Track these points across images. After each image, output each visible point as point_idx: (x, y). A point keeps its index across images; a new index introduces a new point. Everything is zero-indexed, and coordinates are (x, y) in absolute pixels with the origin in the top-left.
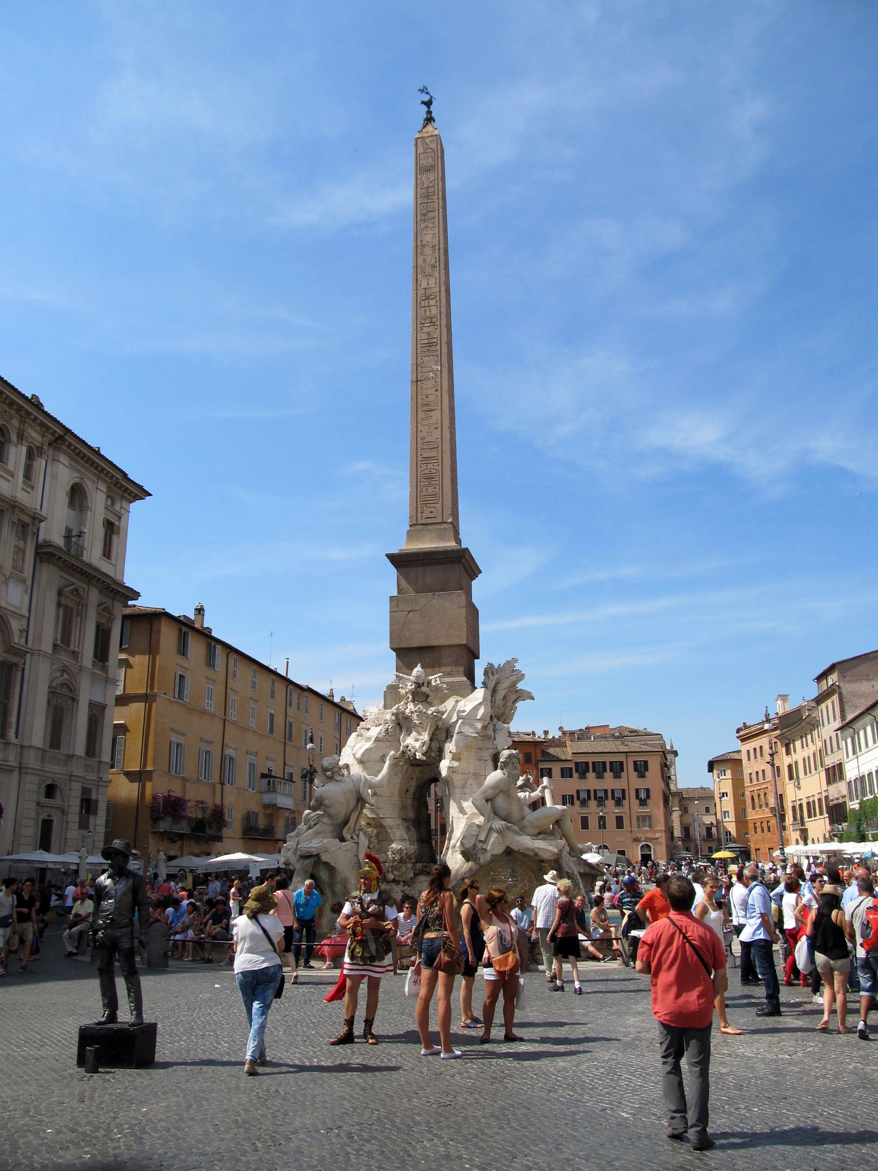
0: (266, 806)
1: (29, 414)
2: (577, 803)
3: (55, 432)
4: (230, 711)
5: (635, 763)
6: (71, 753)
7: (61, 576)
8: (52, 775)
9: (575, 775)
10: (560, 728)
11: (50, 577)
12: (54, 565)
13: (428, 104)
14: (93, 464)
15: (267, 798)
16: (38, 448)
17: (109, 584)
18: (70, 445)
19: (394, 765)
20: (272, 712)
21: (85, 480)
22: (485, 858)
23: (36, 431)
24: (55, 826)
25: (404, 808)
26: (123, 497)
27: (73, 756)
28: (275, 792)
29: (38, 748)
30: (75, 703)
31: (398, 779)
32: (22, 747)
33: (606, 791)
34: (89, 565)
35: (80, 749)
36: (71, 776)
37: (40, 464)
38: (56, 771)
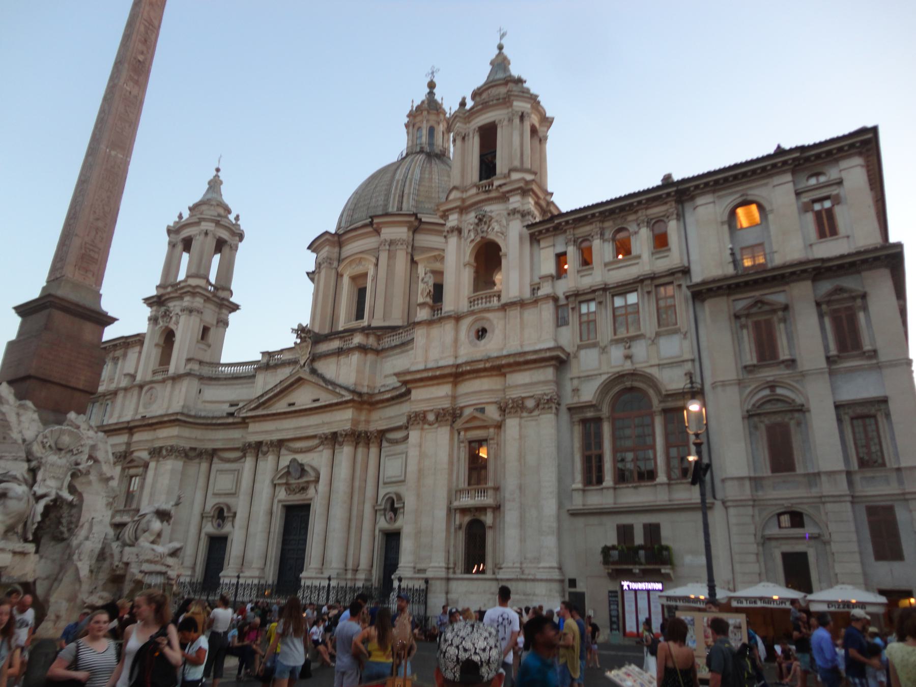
1: (631, 205)
3: (668, 194)
6: (816, 471)
7: (734, 300)
8: (783, 502)
12: (711, 297)
14: (744, 175)
16: (664, 216)
17: (814, 269)
18: (697, 187)
21: (750, 192)
23: (656, 206)
27: (818, 474)
29: (741, 479)
30: (807, 414)
32: (723, 481)
36: (821, 497)
37: (672, 227)
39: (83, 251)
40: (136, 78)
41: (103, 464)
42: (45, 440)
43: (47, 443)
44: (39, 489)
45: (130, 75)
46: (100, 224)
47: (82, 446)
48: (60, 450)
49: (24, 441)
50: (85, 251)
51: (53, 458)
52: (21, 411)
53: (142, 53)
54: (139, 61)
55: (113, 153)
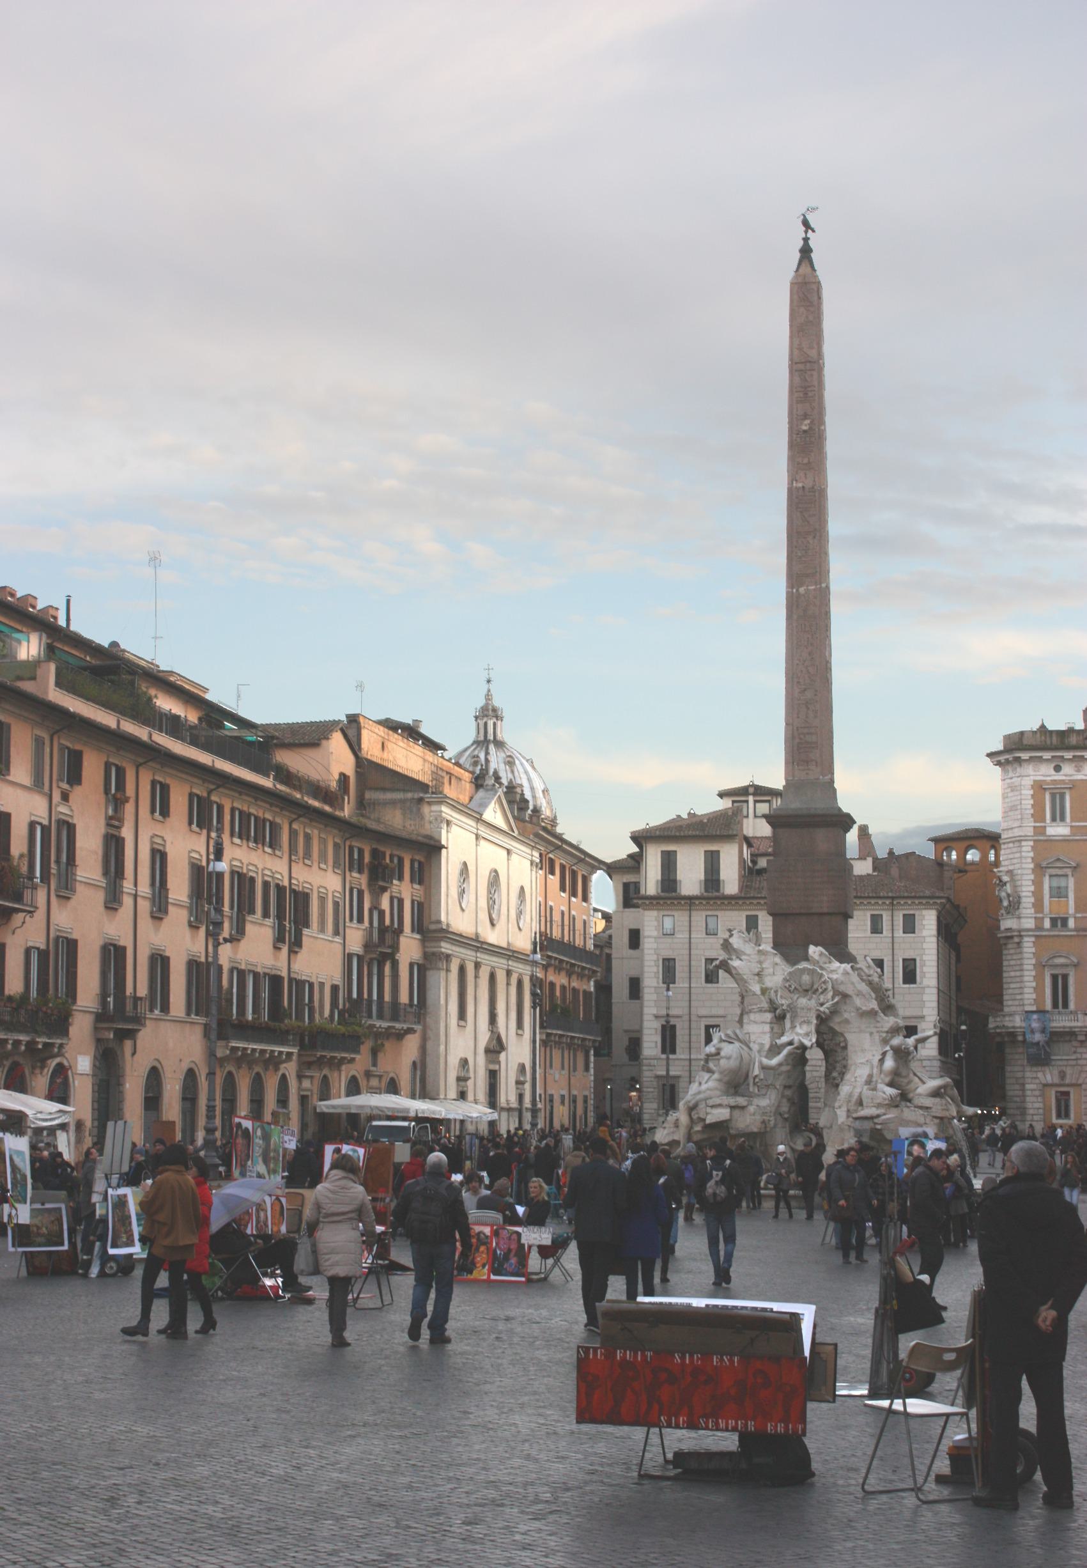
39: (797, 740)
40: (806, 461)
41: (854, 997)
42: (787, 985)
43: (790, 986)
44: (784, 1039)
45: (798, 463)
46: (809, 694)
47: (825, 982)
48: (807, 991)
49: (764, 991)
50: (801, 739)
51: (803, 1001)
52: (763, 958)
53: (805, 416)
54: (805, 431)
55: (802, 590)
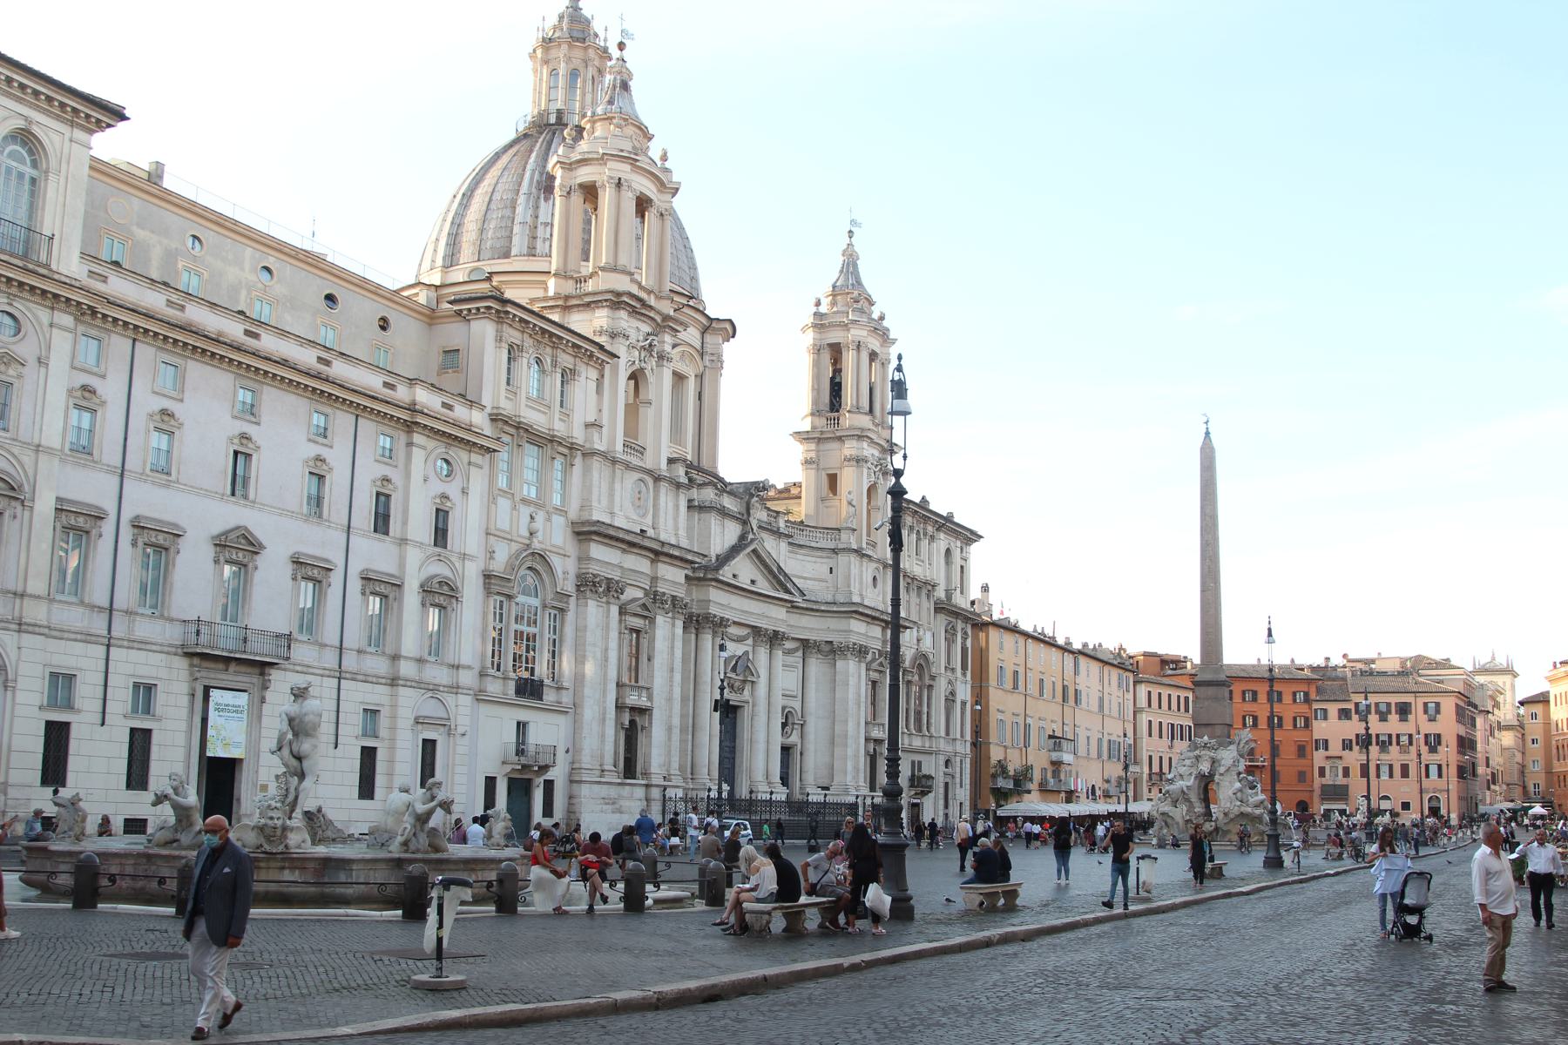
0: (1053, 763)
2: (1356, 748)
4: (1028, 687)
5: (1425, 704)
9: (1355, 717)
10: (1345, 656)
11: (942, 620)
13: (1206, 423)
15: (1055, 756)
19: (1196, 777)
20: (1054, 679)
22: (1232, 816)
24: (950, 786)
25: (1199, 794)
26: (967, 544)
28: (1061, 751)
31: (1197, 782)
33: (1390, 736)
34: (956, 606)
35: (958, 736)
38: (949, 749)
